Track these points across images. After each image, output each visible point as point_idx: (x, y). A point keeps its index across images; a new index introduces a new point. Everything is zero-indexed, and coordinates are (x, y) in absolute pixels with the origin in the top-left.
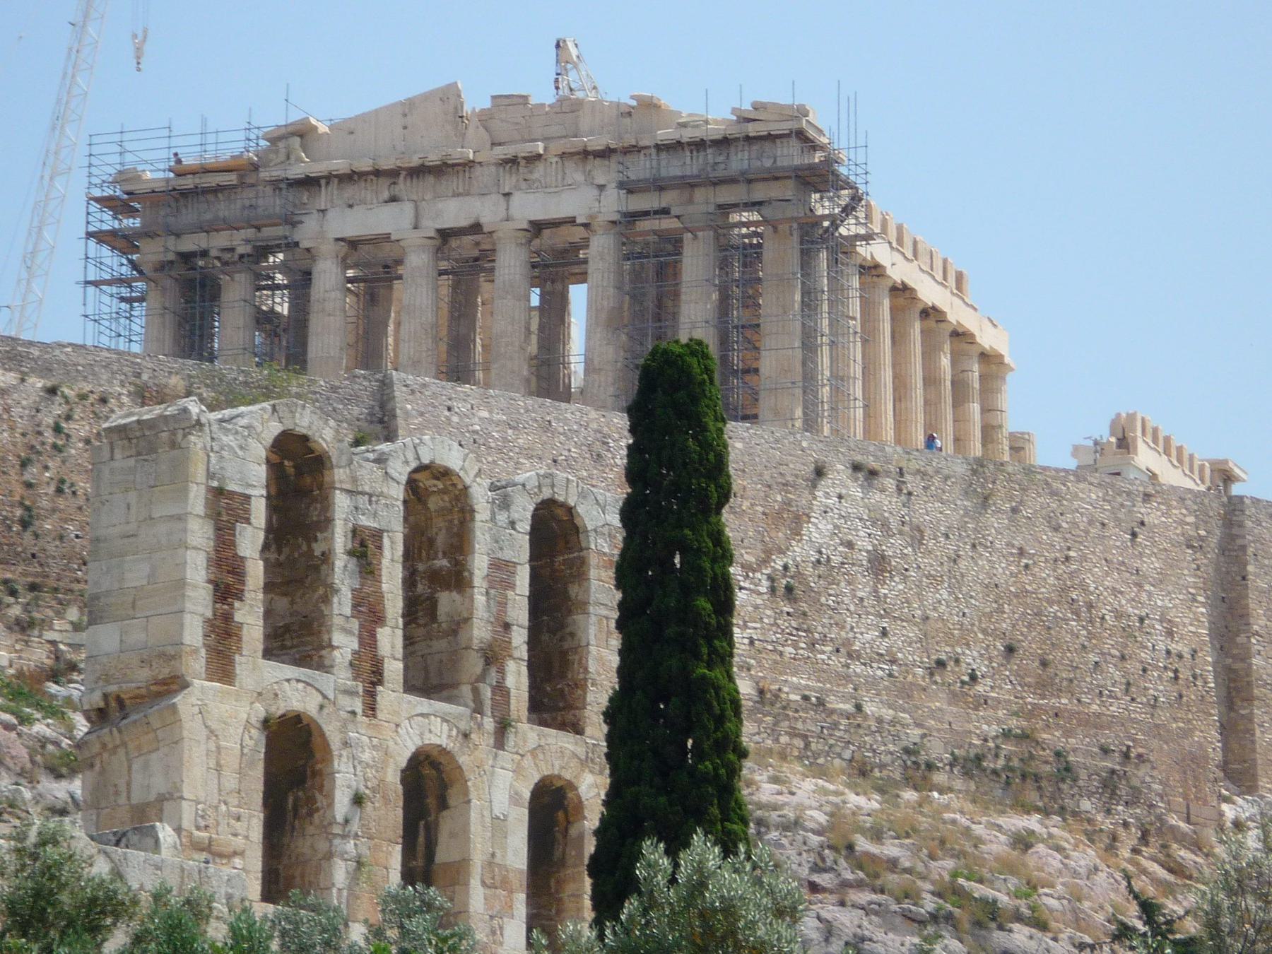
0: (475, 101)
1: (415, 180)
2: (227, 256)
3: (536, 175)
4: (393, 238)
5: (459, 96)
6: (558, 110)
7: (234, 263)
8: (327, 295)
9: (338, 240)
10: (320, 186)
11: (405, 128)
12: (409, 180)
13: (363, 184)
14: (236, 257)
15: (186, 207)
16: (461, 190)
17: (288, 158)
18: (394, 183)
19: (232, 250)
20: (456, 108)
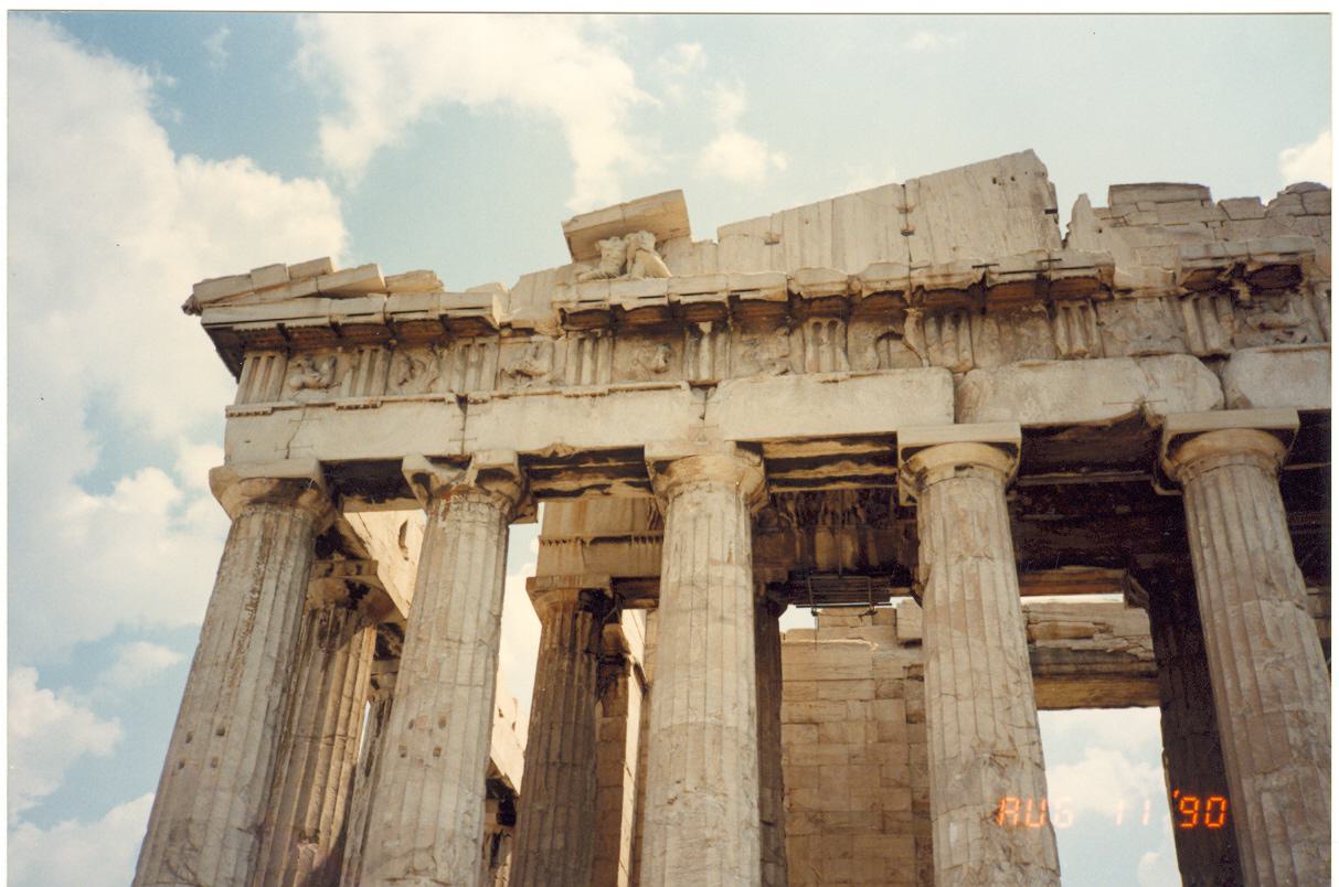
0: (1081, 181)
1: (947, 330)
2: (443, 475)
3: (1290, 318)
4: (904, 441)
5: (1044, 175)
6: (1297, 209)
7: (465, 491)
8: (716, 572)
9: (744, 446)
10: (700, 335)
11: (906, 233)
12: (931, 329)
13: (809, 332)
14: (471, 475)
15: (356, 369)
16: (1079, 345)
17: (623, 270)
18: (889, 336)
19: (460, 463)
20: (1037, 197)
